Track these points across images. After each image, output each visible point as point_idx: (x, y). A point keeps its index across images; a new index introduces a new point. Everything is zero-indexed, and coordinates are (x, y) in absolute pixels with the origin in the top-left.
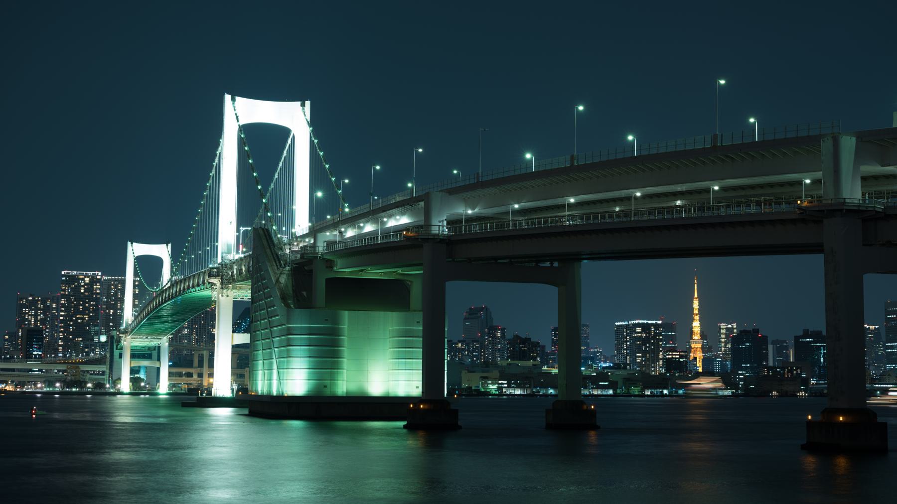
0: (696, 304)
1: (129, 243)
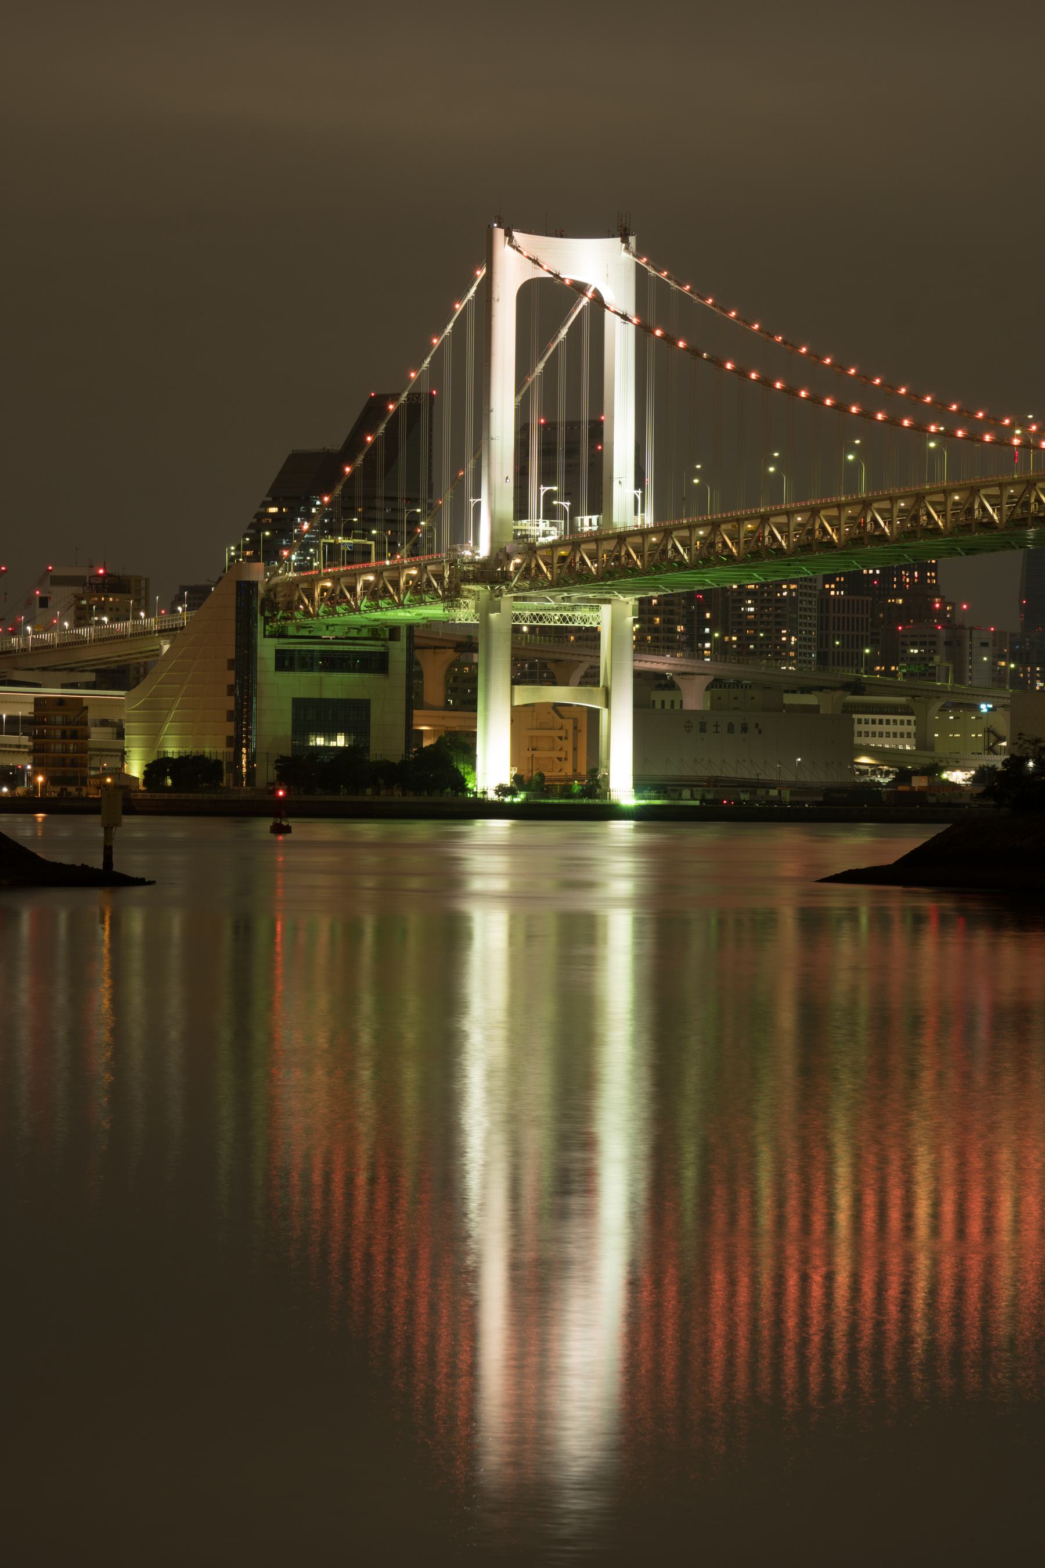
1: (499, 233)
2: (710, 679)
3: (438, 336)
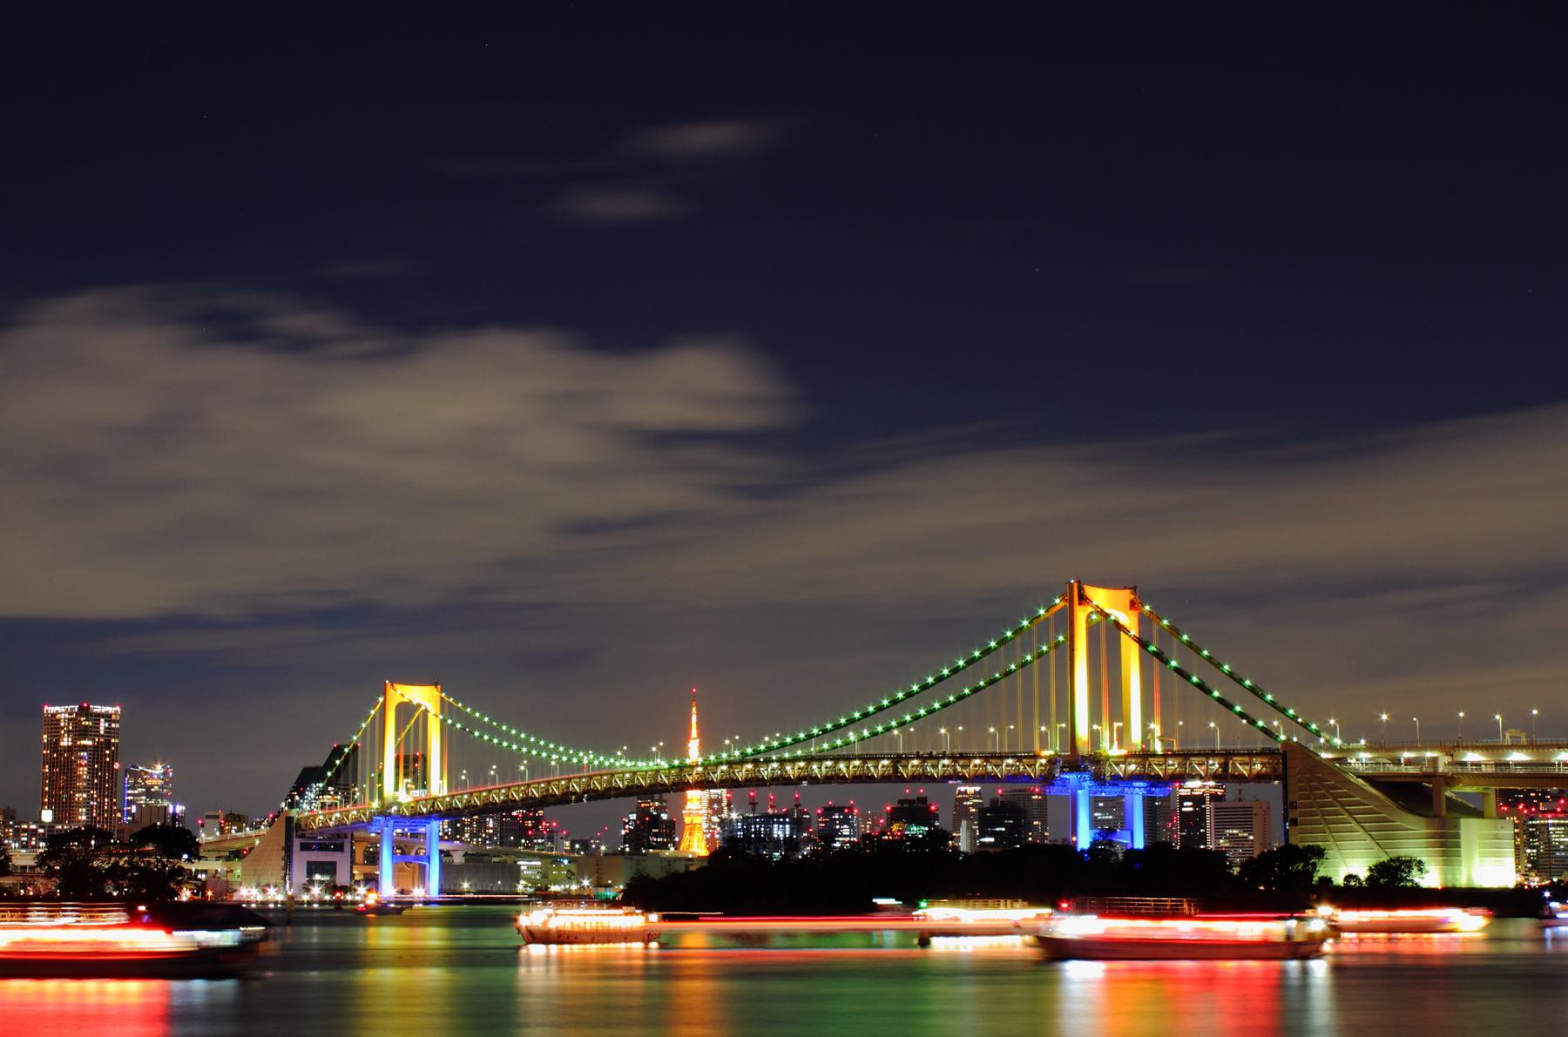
2: (464, 853)
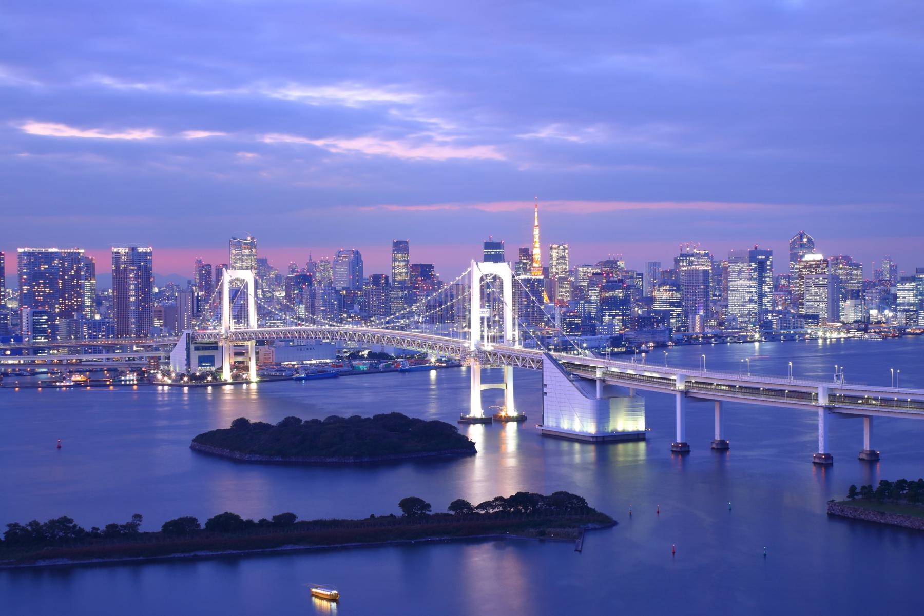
0: (536, 232)
3: (216, 288)
